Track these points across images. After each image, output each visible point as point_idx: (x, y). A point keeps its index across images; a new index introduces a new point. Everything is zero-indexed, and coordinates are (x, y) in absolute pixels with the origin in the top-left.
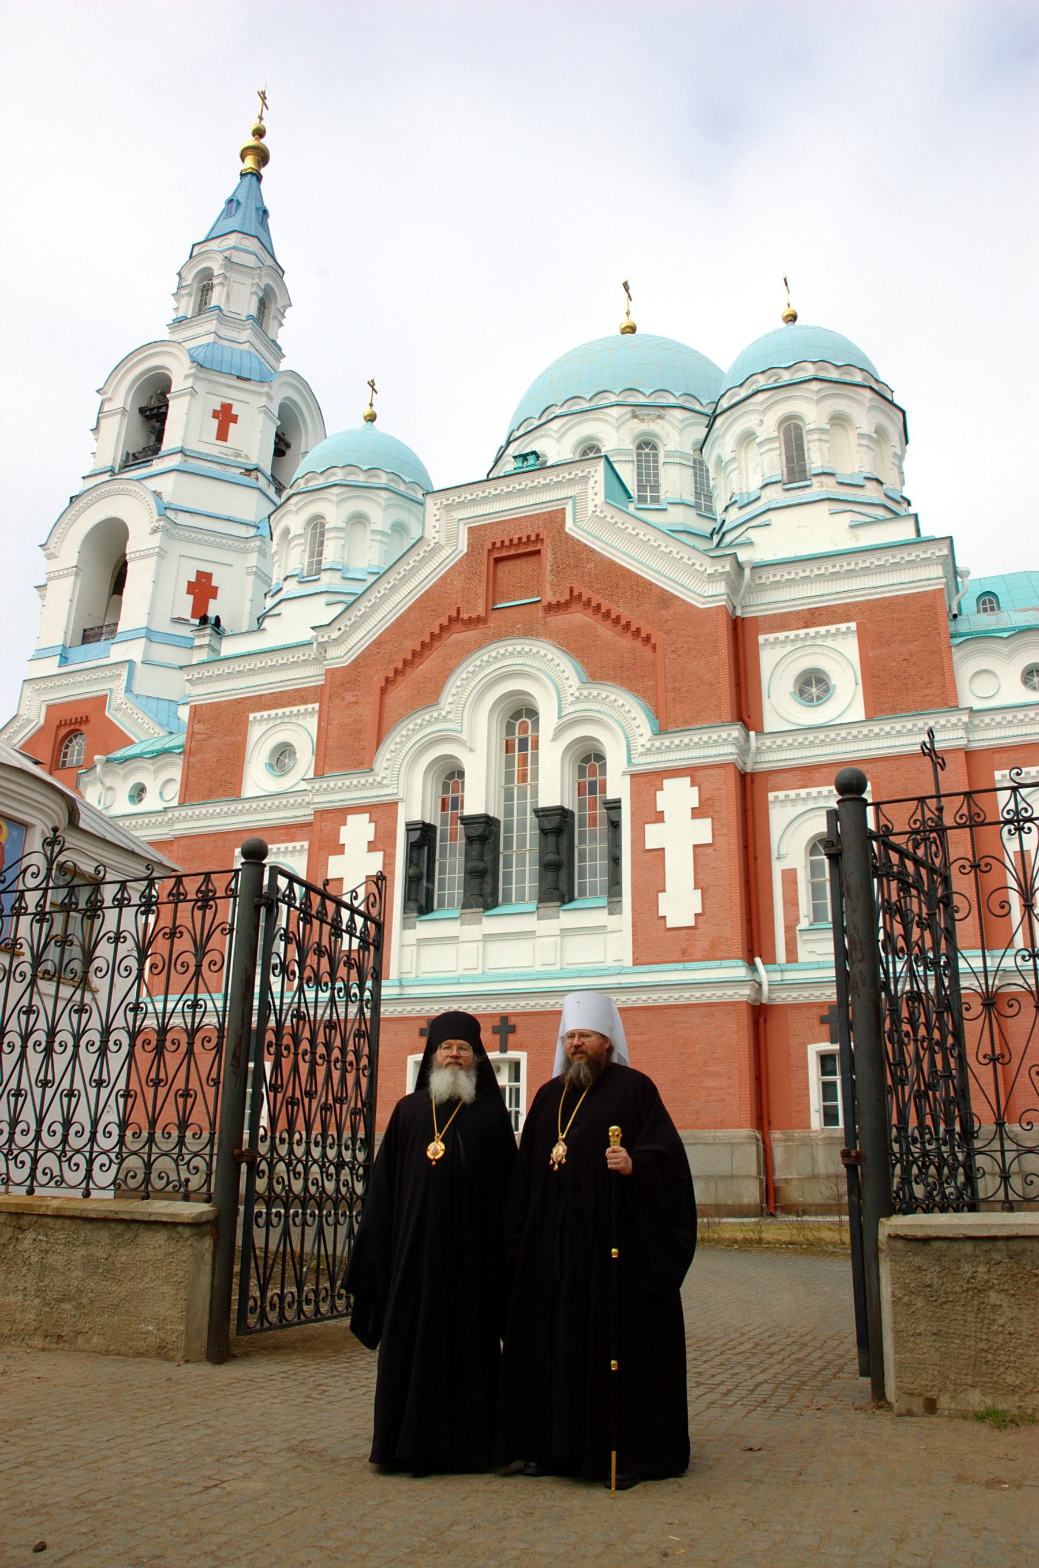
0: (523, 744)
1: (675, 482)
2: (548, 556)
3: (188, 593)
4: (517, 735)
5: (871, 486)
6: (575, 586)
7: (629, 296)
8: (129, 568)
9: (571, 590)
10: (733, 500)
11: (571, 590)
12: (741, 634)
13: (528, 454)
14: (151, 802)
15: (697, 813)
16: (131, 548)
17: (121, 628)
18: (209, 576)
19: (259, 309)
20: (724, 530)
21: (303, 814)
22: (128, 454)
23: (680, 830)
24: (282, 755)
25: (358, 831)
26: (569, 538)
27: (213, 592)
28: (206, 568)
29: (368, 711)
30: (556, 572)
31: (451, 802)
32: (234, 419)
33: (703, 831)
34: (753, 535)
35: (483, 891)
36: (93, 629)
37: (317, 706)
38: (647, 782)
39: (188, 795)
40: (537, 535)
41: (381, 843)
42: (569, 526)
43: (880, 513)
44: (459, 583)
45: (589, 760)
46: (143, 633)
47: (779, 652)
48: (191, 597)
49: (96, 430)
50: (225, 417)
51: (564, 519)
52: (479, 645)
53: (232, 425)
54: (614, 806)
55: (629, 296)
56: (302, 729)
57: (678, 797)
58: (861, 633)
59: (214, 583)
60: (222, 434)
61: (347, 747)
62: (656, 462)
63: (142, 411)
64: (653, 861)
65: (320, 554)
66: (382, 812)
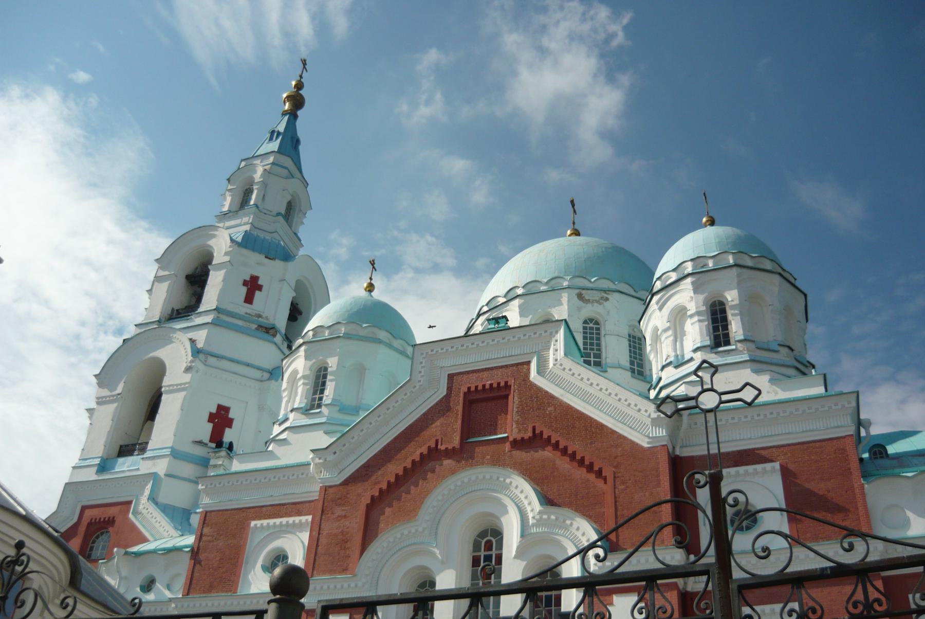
1: (615, 349)
2: (514, 401)
3: (209, 421)
4: (482, 553)
5: (784, 351)
6: (537, 425)
7: (575, 211)
8: (164, 397)
9: (534, 428)
10: (668, 361)
11: (534, 428)
13: (499, 318)
16: (166, 382)
17: (150, 447)
18: (227, 409)
19: (287, 209)
20: (661, 385)
22: (173, 309)
26: (533, 386)
27: (229, 423)
28: (225, 403)
29: (355, 524)
30: (522, 412)
32: (260, 288)
36: (127, 446)
37: (310, 518)
39: (189, 589)
40: (506, 383)
42: (533, 375)
43: (792, 372)
46: (168, 452)
48: (210, 426)
49: (150, 291)
50: (253, 286)
51: (529, 369)
53: (257, 293)
55: (575, 211)
59: (231, 415)
60: (249, 299)
62: (599, 334)
65: (322, 392)
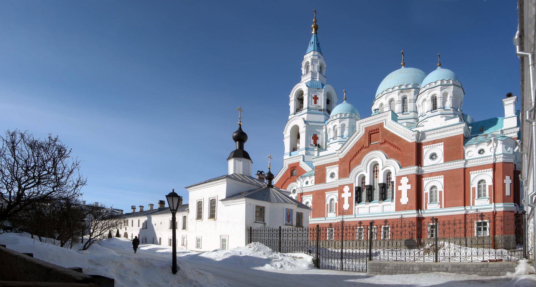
0: (376, 171)
2: (380, 133)
12: (419, 147)
14: (309, 184)
15: (408, 183)
21: (337, 186)
23: (405, 187)
24: (332, 175)
25: (346, 189)
29: (347, 166)
30: (382, 136)
31: (363, 182)
33: (409, 187)
34: (424, 124)
35: (370, 199)
38: (399, 178)
39: (316, 183)
41: (351, 191)
43: (452, 116)
44: (363, 140)
45: (388, 174)
47: (427, 149)
50: (316, 98)
52: (368, 152)
54: (393, 182)
56: (335, 170)
57: (405, 180)
58: (444, 144)
60: (315, 103)
61: (345, 173)
63: (298, 99)
64: (399, 193)
66: (351, 186)
